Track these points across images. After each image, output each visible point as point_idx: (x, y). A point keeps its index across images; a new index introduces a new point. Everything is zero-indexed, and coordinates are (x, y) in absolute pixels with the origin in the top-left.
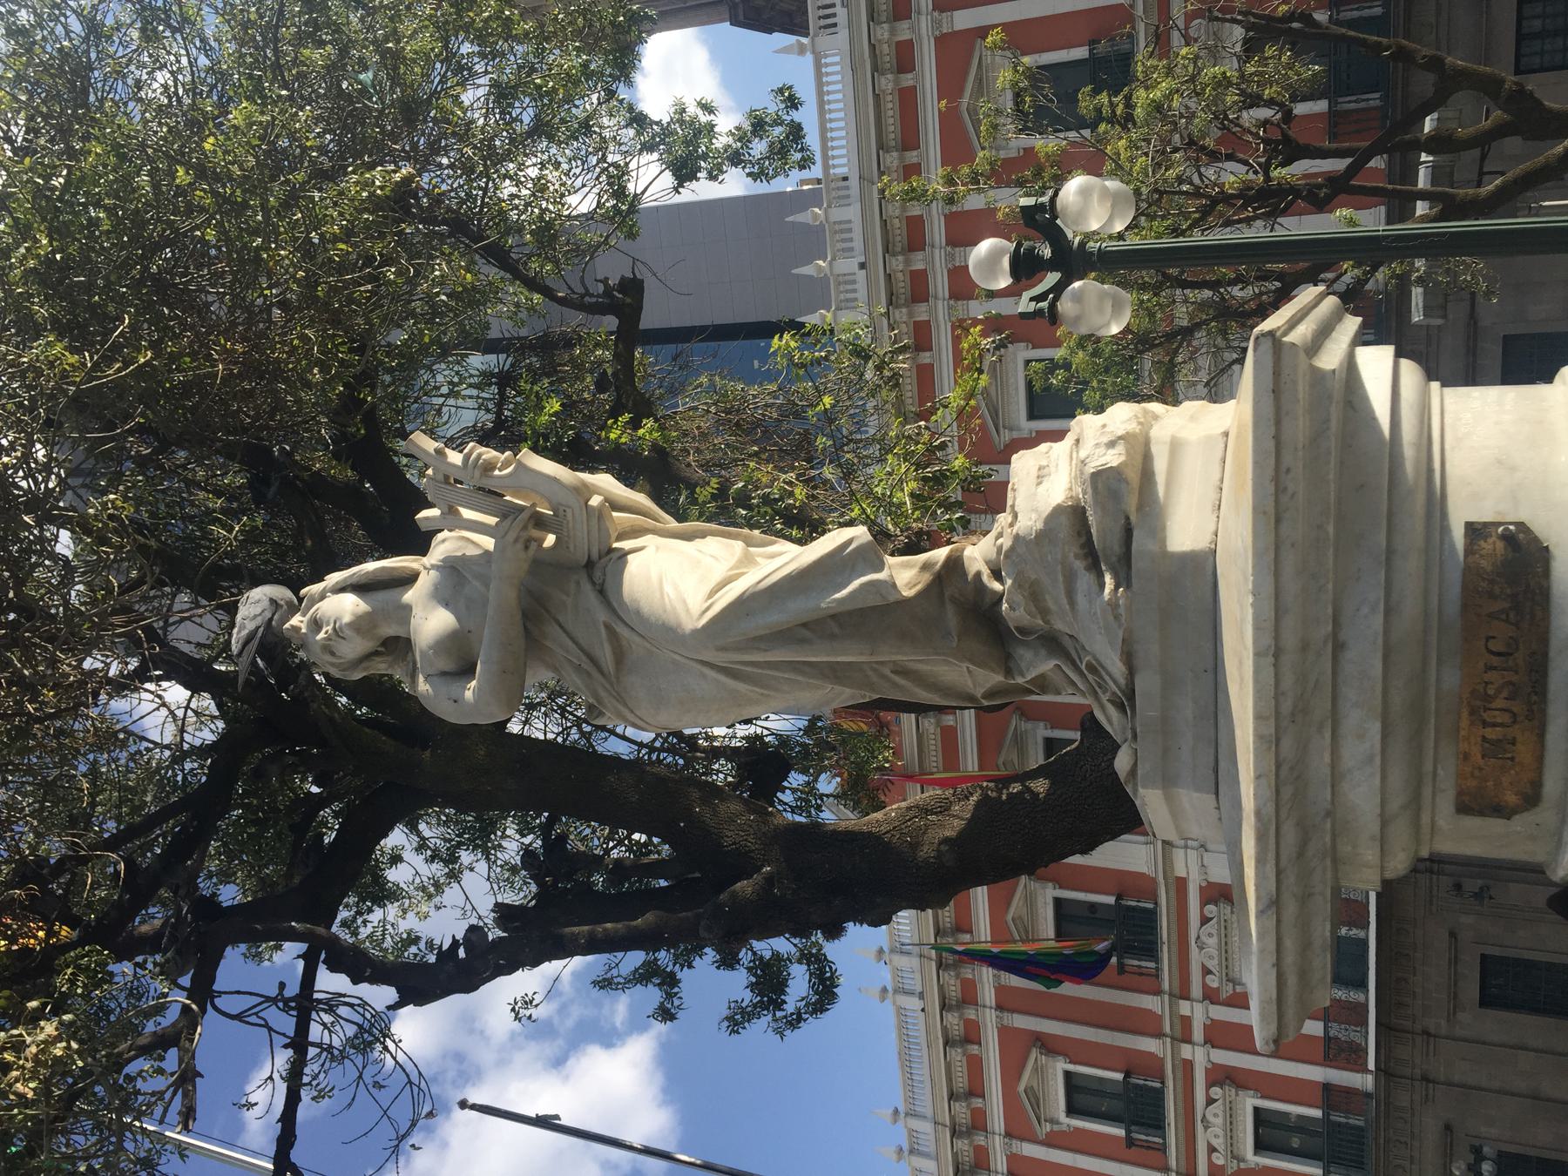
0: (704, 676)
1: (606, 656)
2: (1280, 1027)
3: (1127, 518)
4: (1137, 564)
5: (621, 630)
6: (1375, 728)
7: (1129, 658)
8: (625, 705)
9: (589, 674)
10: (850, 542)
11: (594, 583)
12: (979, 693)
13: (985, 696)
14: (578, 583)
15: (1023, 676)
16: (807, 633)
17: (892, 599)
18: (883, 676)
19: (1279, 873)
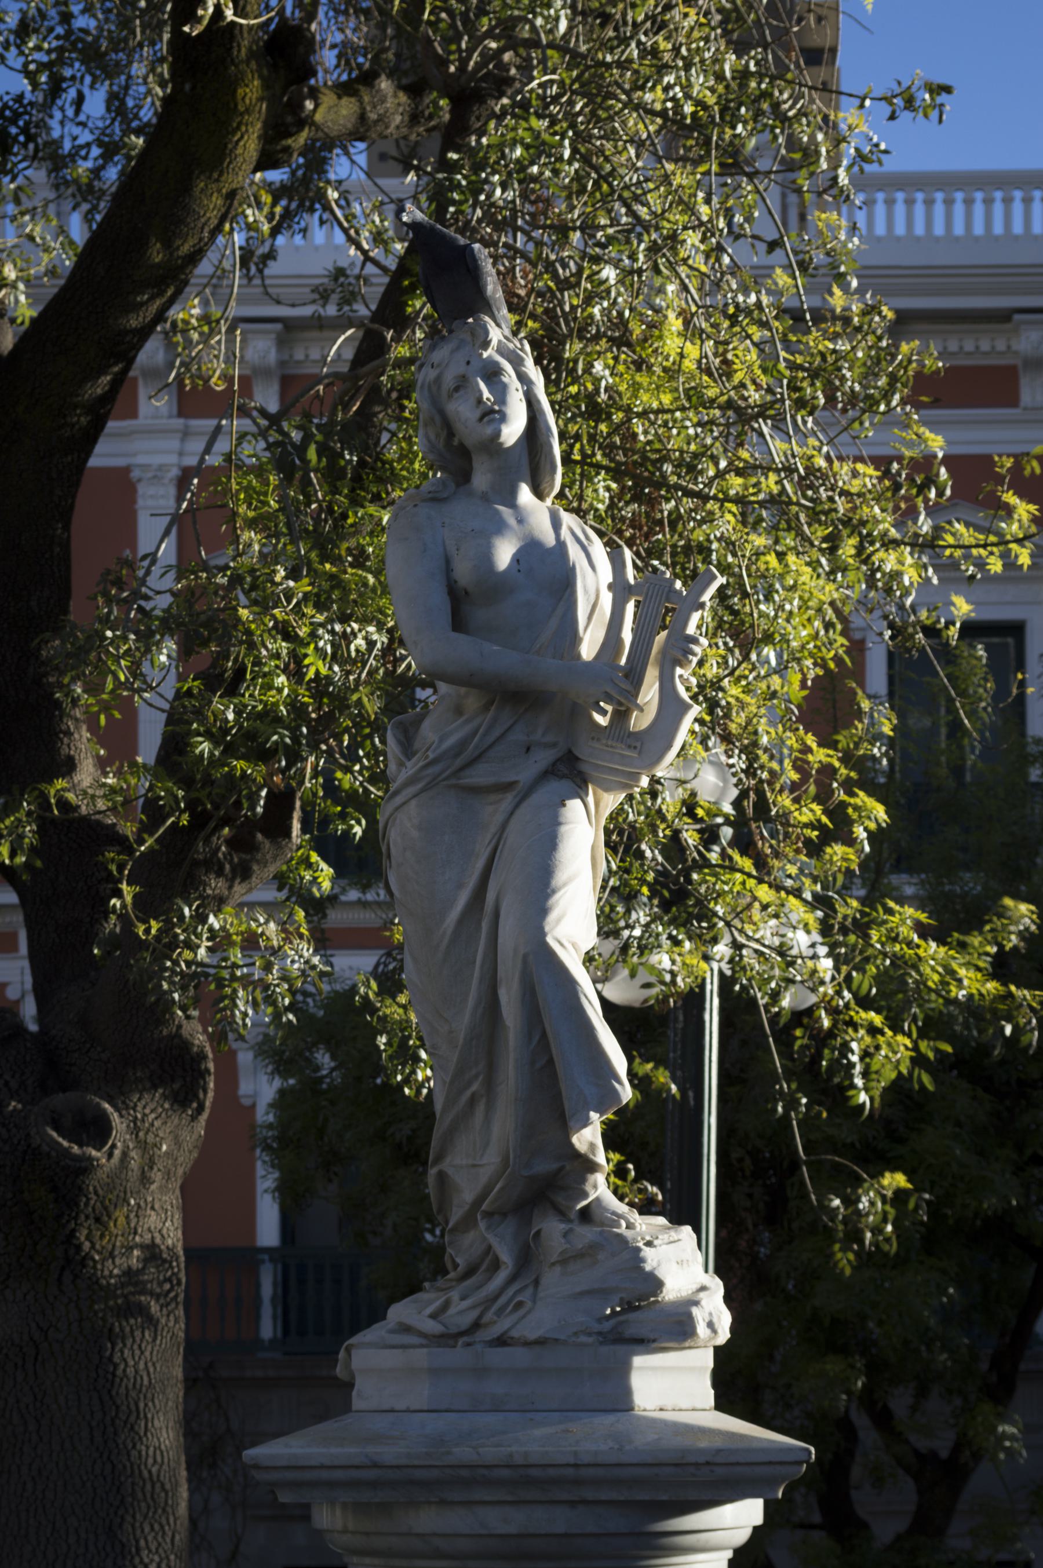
0: (460, 886)
1: (481, 775)
2: (267, 1468)
3: (654, 1341)
4: (621, 1349)
5: (508, 800)
6: (512, 1529)
7: (540, 1342)
8: (423, 790)
9: (458, 755)
10: (620, 1083)
11: (554, 764)
12: (445, 1165)
13: (442, 1176)
14: (554, 745)
15: (488, 1228)
16: (536, 1039)
17: (571, 1124)
18: (469, 1084)
19: (398, 1467)
